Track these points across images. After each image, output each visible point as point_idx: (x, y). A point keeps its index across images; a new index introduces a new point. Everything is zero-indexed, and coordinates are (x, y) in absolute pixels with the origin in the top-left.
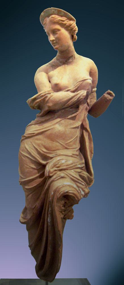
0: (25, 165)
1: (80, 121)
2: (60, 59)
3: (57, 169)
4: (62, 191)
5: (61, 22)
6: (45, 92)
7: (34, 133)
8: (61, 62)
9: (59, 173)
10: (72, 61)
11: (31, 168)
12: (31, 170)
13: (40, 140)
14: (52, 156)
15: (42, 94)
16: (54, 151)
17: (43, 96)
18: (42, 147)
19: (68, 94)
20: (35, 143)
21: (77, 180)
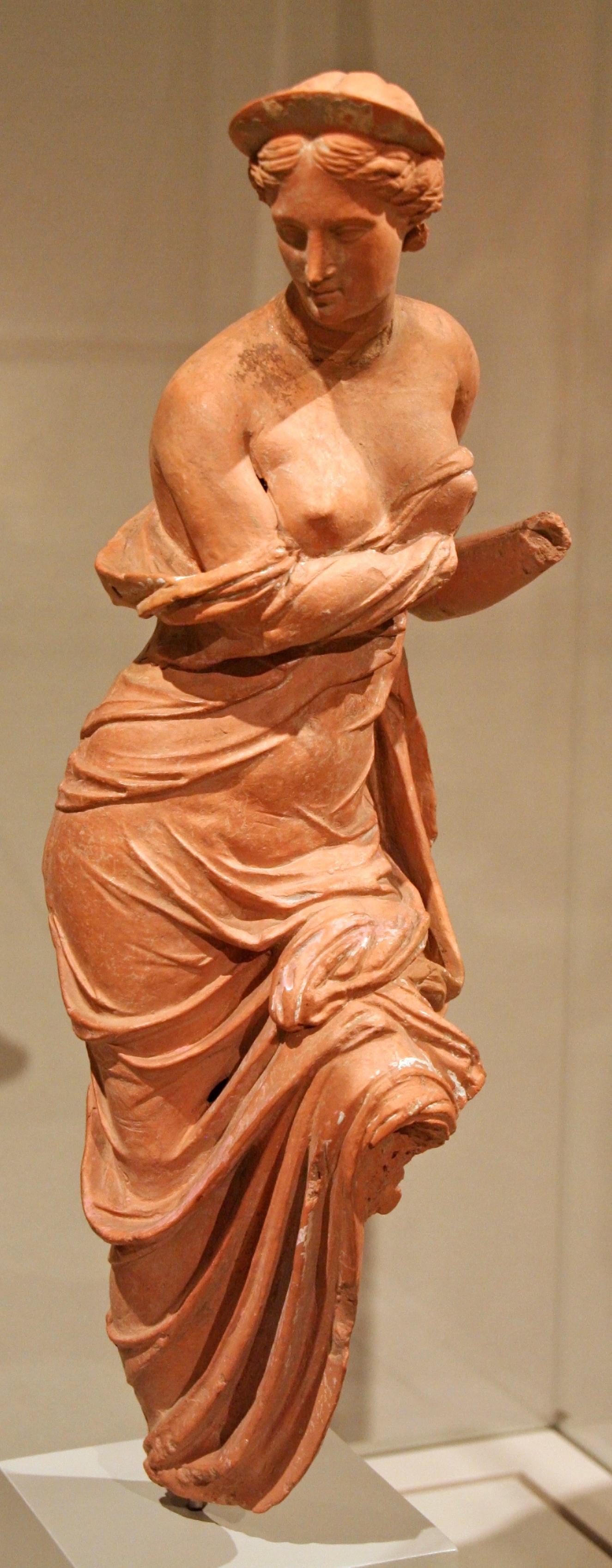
0: (134, 948)
1: (385, 678)
3: (342, 986)
4: (396, 1112)
6: (259, 570)
9: (354, 1005)
11: (165, 961)
12: (170, 971)
13: (209, 809)
15: (249, 581)
16: (279, 861)
17: (248, 590)
18: (222, 846)
20: (187, 830)
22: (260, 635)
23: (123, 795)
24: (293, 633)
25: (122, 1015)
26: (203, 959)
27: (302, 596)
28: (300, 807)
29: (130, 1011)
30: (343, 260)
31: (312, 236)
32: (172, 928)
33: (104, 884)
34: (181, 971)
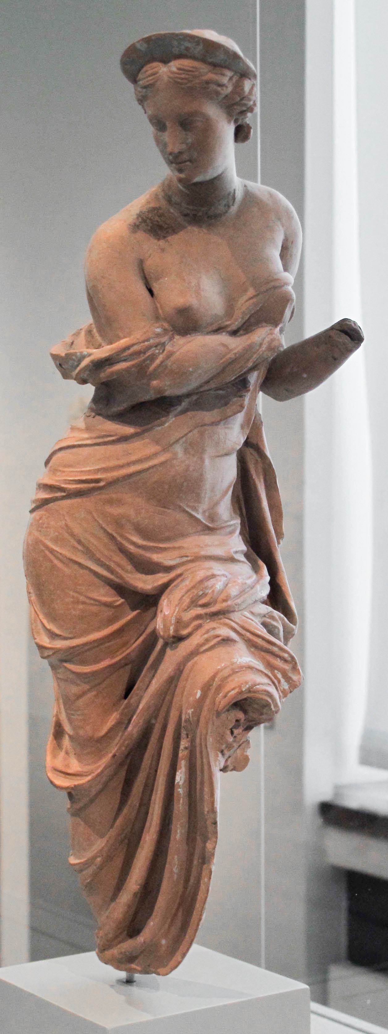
2: (183, 204)
6: (144, 342)
7: (97, 481)
8: (186, 215)
9: (209, 625)
11: (92, 602)
12: (94, 609)
14: (172, 563)
16: (168, 539)
17: (138, 353)
19: (224, 345)
22: (148, 385)
23: (63, 494)
24: (168, 383)
25: (66, 639)
26: (117, 601)
27: (172, 359)
28: (181, 504)
29: (70, 636)
30: (190, 140)
31: (168, 124)
32: (96, 580)
33: (52, 551)
34: (104, 608)
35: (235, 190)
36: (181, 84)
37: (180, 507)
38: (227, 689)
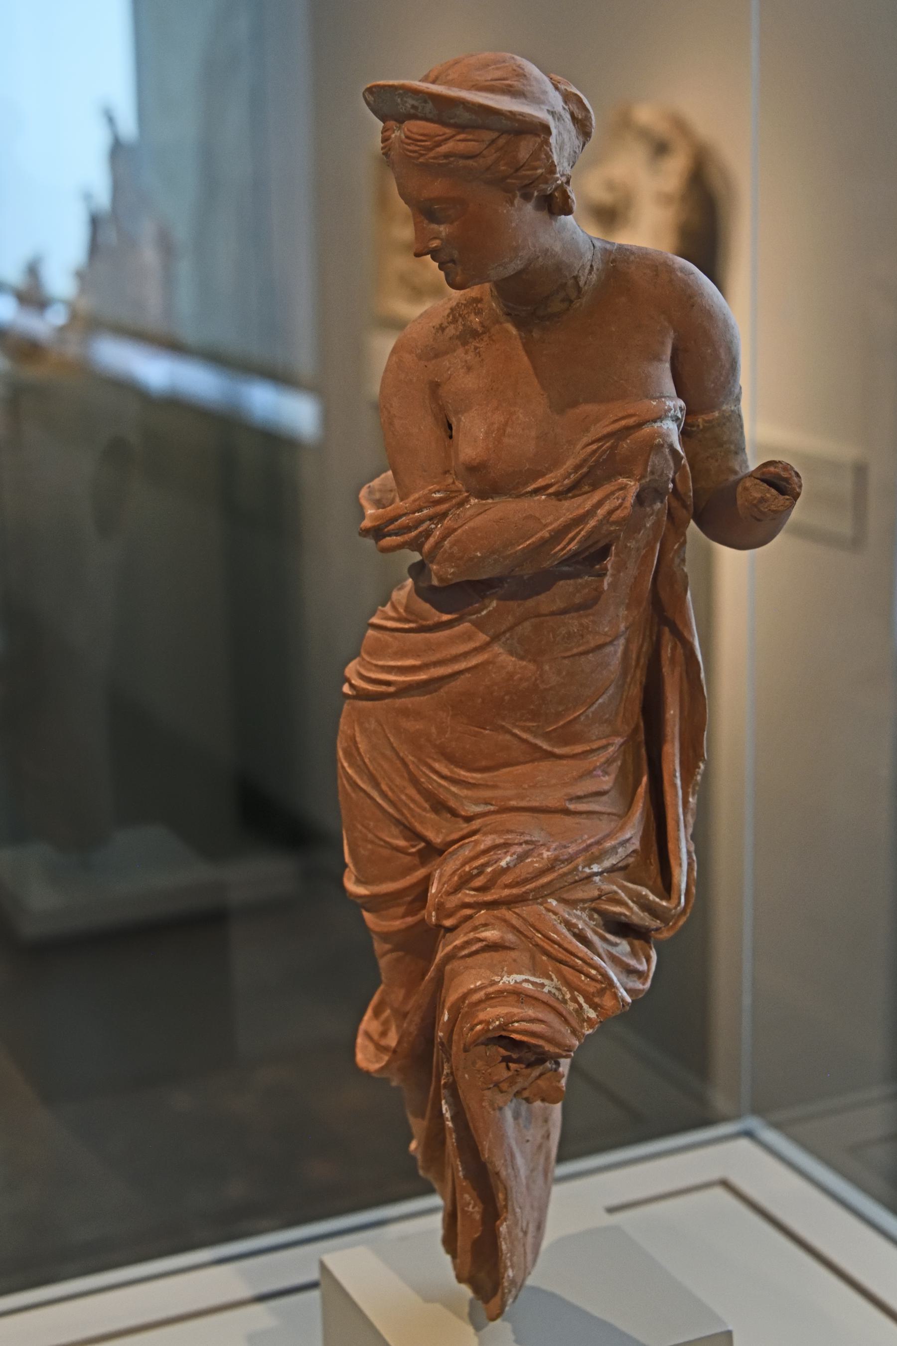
5: (462, 162)
7: (388, 683)
10: (568, 309)
11: (382, 843)
13: (416, 714)
17: (408, 529)
21: (562, 955)
28: (504, 724)
29: (363, 880)
35: (576, 278)
36: (414, 158)
37: (503, 727)
38: (482, 1016)
